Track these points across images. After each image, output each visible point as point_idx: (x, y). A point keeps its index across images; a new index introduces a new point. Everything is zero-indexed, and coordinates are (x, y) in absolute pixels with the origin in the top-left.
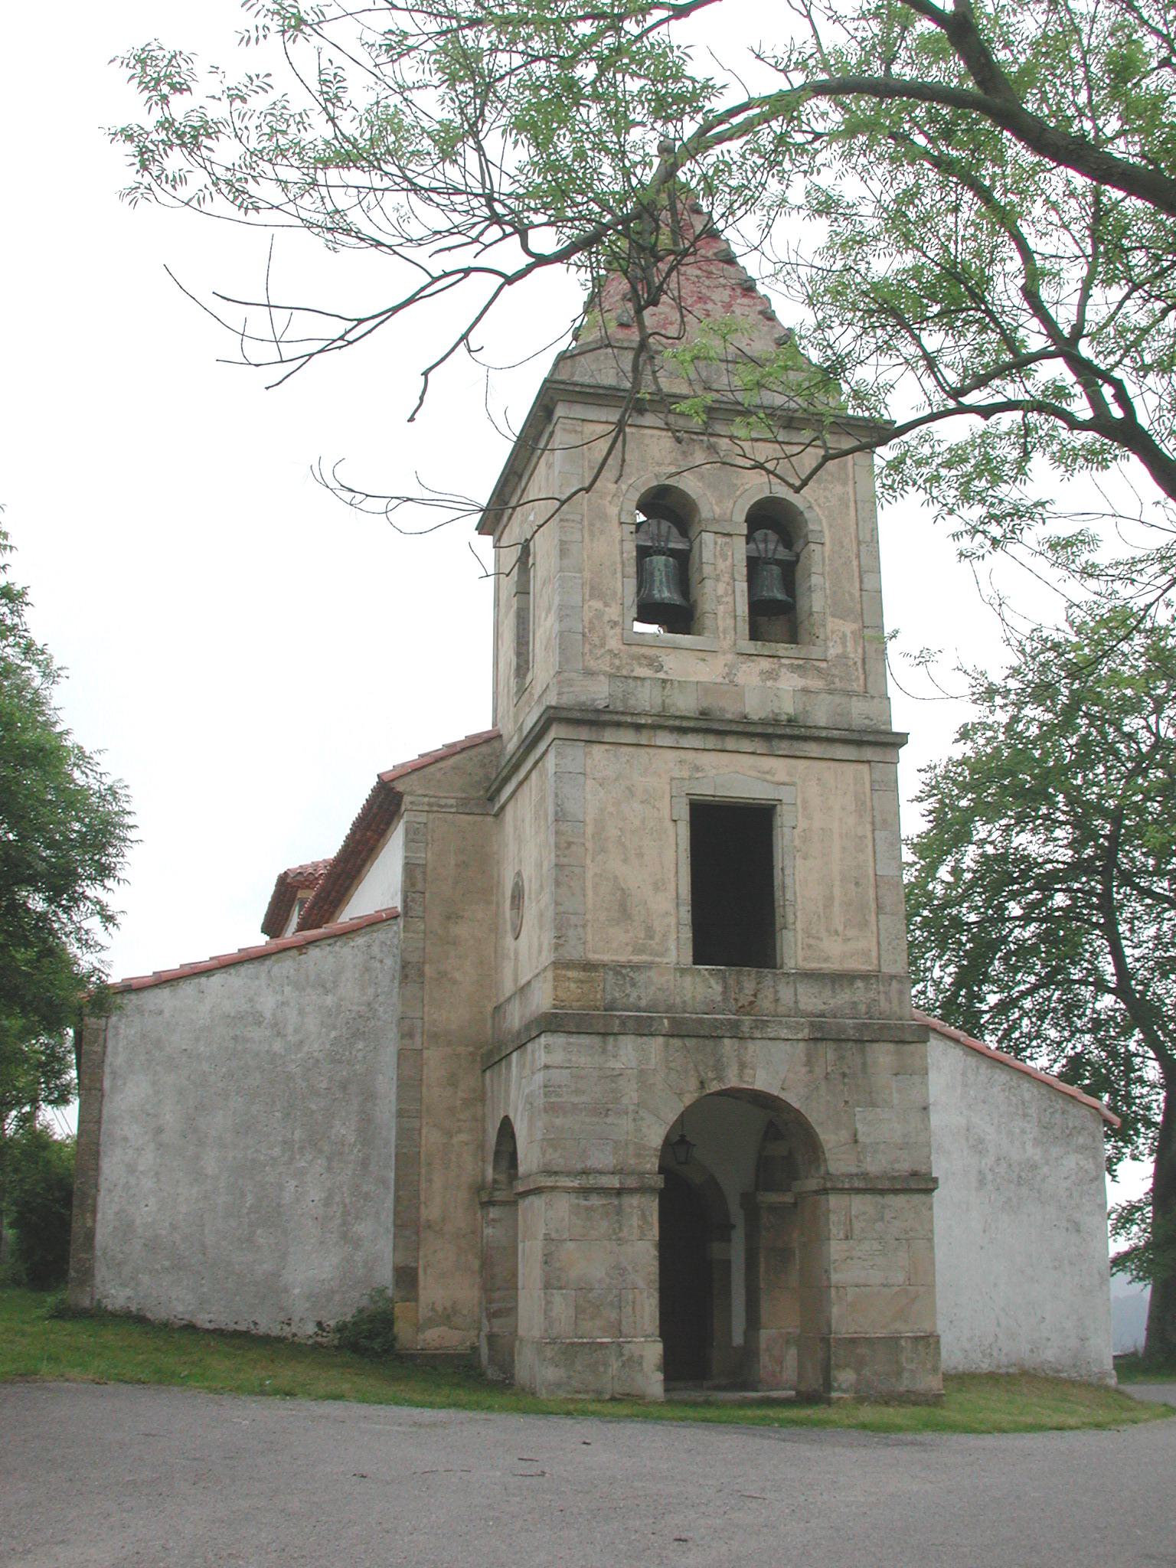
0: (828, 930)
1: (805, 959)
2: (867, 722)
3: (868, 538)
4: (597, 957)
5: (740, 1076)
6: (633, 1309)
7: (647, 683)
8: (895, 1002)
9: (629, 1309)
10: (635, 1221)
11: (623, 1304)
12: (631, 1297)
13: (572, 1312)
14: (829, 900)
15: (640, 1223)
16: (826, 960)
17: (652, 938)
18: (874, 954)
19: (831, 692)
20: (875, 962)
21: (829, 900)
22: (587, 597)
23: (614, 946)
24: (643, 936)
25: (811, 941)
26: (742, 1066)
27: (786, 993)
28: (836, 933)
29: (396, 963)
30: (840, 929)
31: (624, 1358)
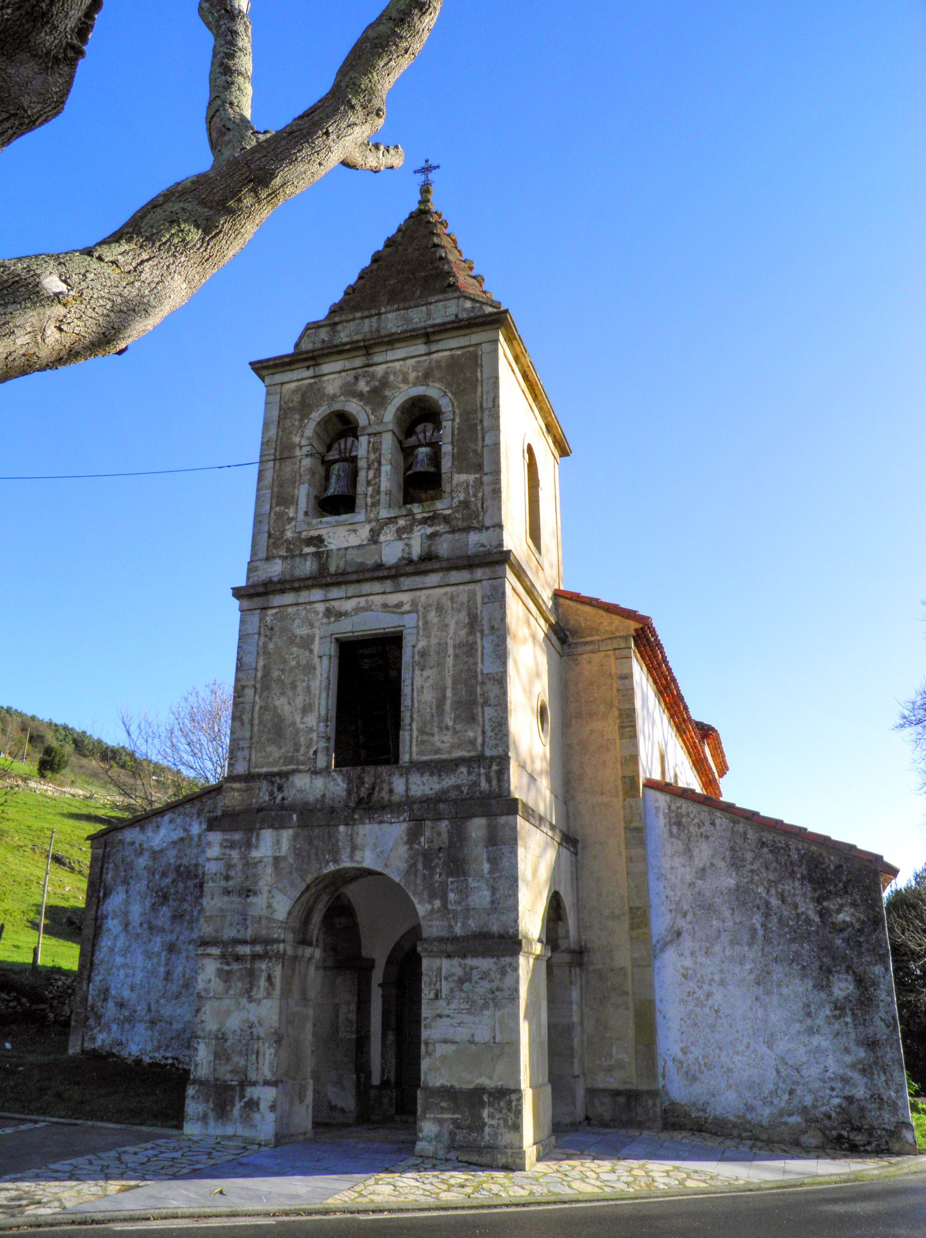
0: (439, 727)
1: (421, 753)
2: (481, 549)
3: (490, 405)
4: (257, 770)
5: (351, 857)
6: (257, 1057)
7: (309, 558)
8: (494, 783)
9: (254, 1057)
10: (263, 983)
11: (250, 1052)
12: (256, 1046)
13: (211, 1057)
14: (441, 701)
15: (267, 984)
16: (438, 751)
17: (297, 751)
18: (480, 740)
19: (453, 531)
20: (480, 748)
21: (441, 701)
22: (274, 505)
23: (271, 760)
24: (292, 750)
25: (425, 738)
26: (354, 848)
27: (399, 785)
28: (447, 728)
29: (239, 805)
30: (450, 724)
31: (246, 1099)
